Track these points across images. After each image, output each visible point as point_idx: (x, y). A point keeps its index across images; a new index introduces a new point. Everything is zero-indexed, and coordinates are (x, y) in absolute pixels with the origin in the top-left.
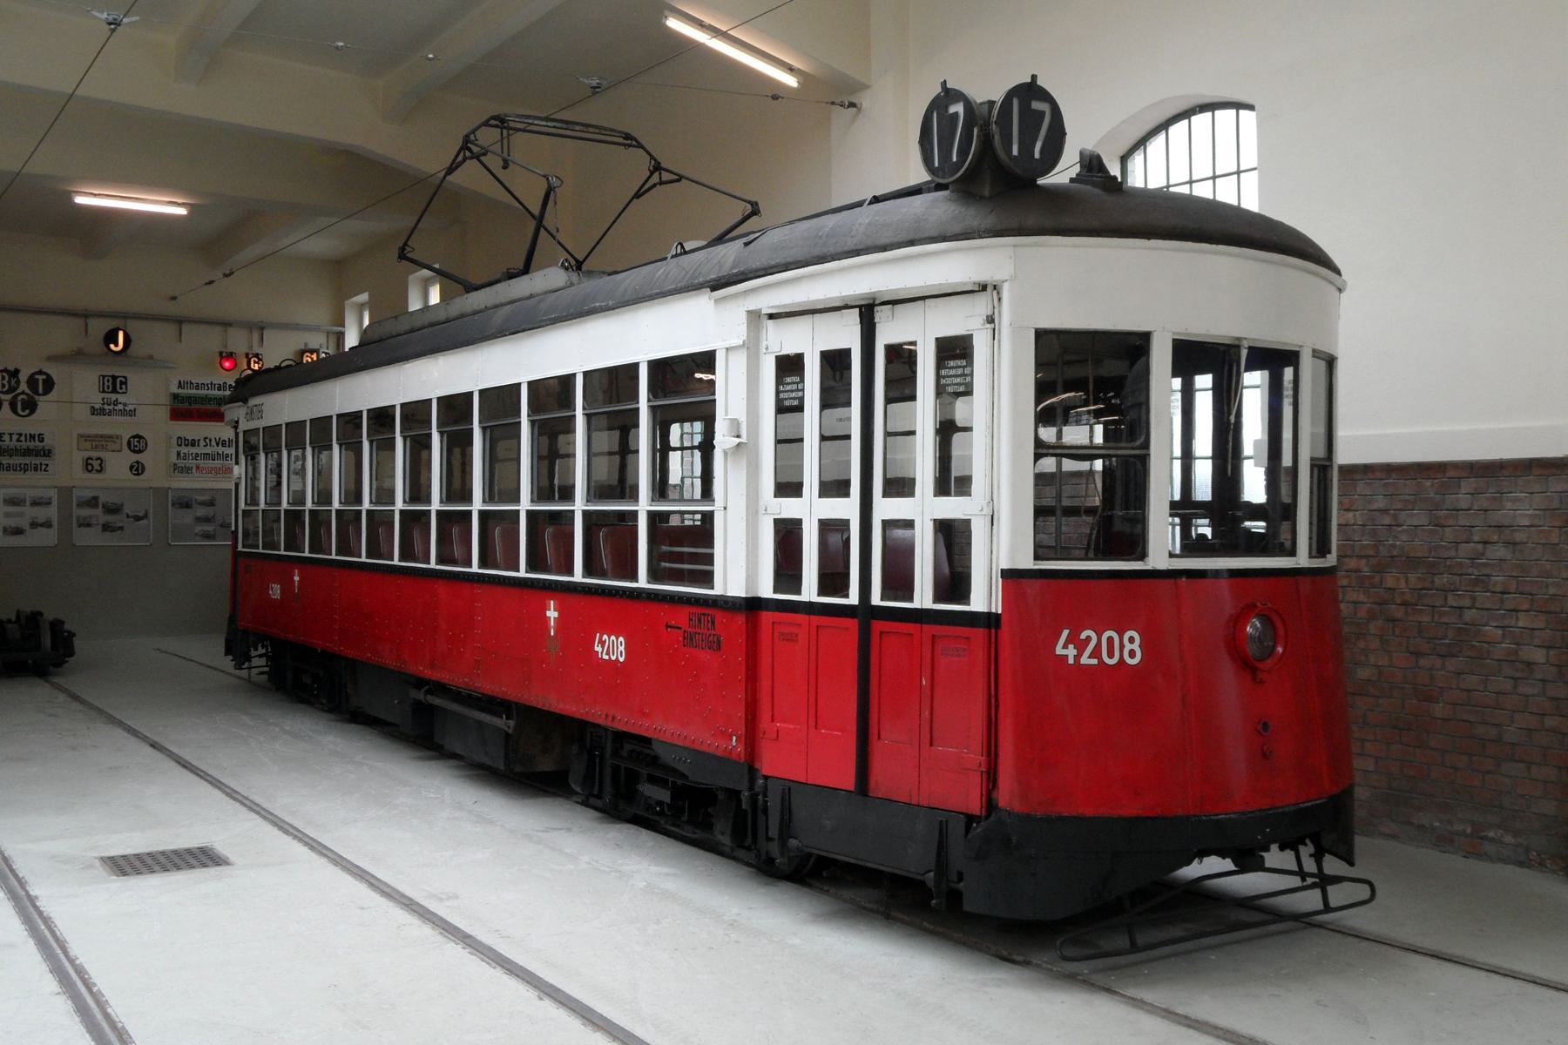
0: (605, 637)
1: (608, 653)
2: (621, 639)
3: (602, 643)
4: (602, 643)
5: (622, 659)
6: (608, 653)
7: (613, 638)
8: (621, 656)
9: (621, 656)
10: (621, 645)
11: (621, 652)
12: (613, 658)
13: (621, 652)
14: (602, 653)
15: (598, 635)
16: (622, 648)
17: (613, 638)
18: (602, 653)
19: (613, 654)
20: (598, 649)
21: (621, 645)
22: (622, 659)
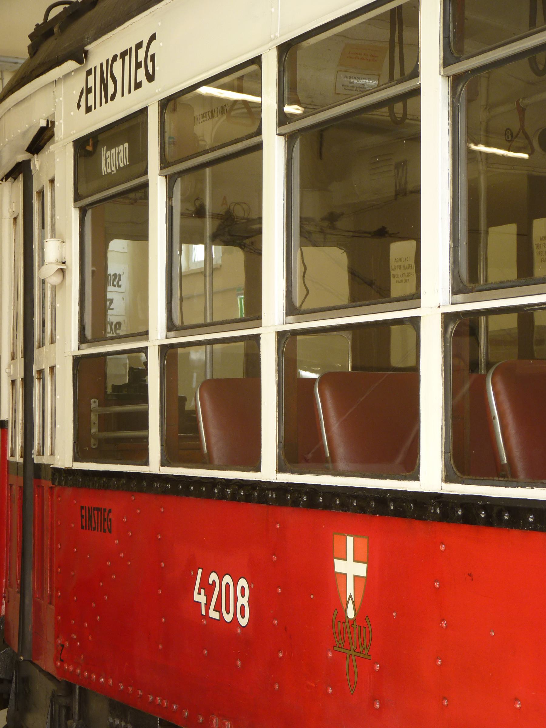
0: (213, 577)
1: (218, 608)
2: (242, 582)
3: (209, 589)
4: (209, 589)
5: (243, 622)
6: (218, 608)
7: (227, 579)
8: (243, 616)
9: (243, 616)
10: (243, 595)
11: (243, 606)
12: (228, 618)
13: (243, 606)
14: (208, 606)
15: (200, 571)
16: (244, 601)
17: (227, 579)
18: (208, 606)
19: (228, 612)
20: (201, 598)
21: (243, 595)
22: (243, 622)
